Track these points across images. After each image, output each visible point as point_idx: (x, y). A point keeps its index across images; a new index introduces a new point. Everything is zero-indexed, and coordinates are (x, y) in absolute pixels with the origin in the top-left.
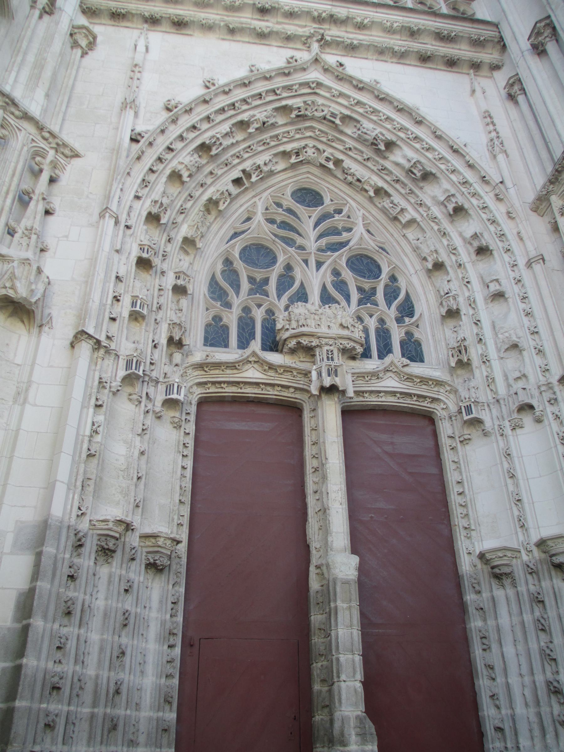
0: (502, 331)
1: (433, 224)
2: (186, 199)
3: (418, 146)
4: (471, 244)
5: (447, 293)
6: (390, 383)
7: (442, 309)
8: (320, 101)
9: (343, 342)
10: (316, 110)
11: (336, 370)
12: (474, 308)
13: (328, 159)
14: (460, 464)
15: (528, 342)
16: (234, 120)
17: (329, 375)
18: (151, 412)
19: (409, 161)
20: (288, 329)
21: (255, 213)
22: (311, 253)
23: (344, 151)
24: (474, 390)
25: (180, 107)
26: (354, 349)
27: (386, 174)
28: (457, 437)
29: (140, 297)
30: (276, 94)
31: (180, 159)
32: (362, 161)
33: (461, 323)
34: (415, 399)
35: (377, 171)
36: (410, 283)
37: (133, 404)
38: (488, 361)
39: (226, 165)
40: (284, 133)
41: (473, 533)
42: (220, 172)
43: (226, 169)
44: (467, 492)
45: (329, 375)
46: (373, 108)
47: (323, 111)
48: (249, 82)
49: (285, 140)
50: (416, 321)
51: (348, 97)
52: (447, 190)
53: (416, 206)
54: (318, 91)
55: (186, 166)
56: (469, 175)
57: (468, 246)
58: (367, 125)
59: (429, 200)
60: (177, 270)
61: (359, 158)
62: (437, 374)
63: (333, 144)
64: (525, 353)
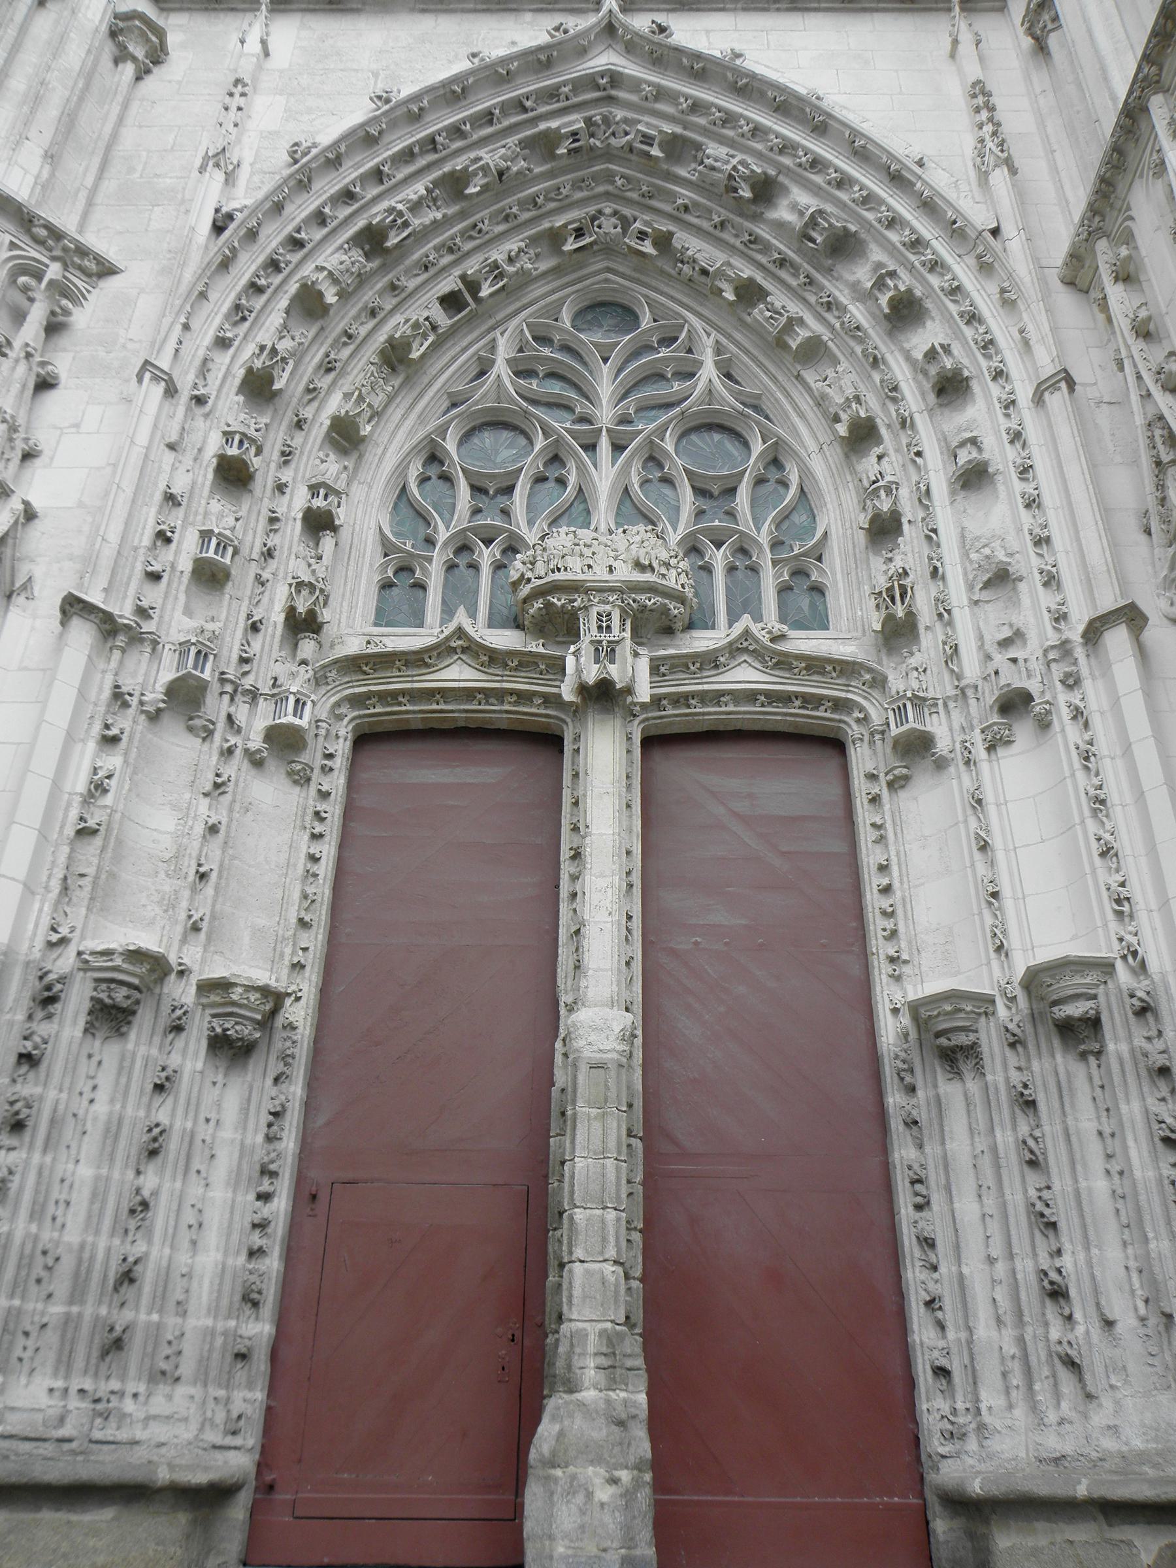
0: (978, 545)
1: (852, 343)
2: (336, 341)
3: (818, 179)
4: (925, 373)
6: (746, 675)
7: (862, 516)
8: (619, 114)
9: (642, 597)
10: (613, 134)
11: (613, 650)
12: (927, 507)
13: (642, 236)
15: (1028, 563)
16: (436, 174)
17: (597, 661)
18: (238, 752)
19: (801, 214)
20: (529, 580)
21: (493, 362)
22: (600, 429)
23: (675, 213)
24: (915, 674)
25: (314, 151)
26: (665, 611)
27: (759, 251)
28: (882, 775)
29: (216, 531)
30: (525, 110)
31: (320, 262)
32: (711, 229)
34: (798, 703)
35: (742, 247)
36: (806, 473)
37: (197, 736)
39: (426, 268)
40: (547, 191)
42: (412, 284)
43: (425, 276)
44: (896, 885)
45: (597, 661)
46: (727, 112)
47: (626, 134)
48: (463, 90)
49: (552, 205)
50: (815, 546)
51: (671, 96)
52: (879, 265)
53: (819, 309)
54: (614, 92)
55: (331, 273)
56: (925, 228)
57: (920, 377)
58: (714, 150)
59: (846, 292)
60: (314, 481)
61: (706, 225)
62: (846, 650)
63: (654, 203)
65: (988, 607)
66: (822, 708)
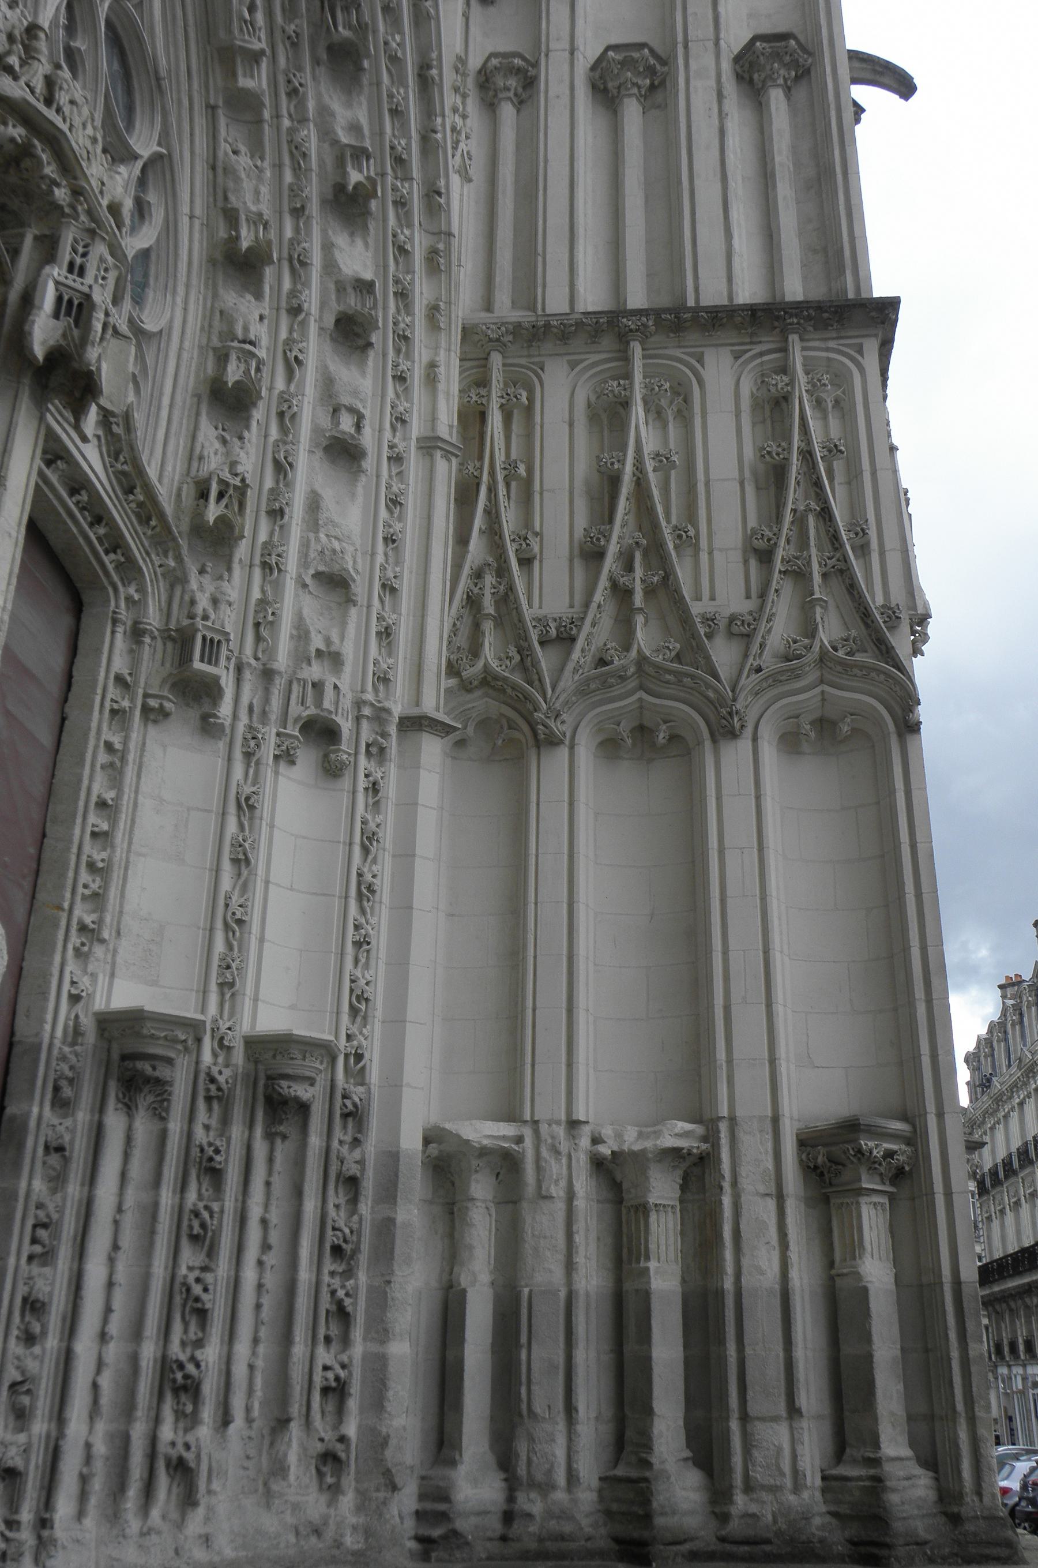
1: (287, 160)
4: (340, 288)
5: (251, 343)
14: (123, 759)
33: (246, 434)
38: (280, 570)
41: (99, 951)
44: (119, 837)
53: (281, 79)
64: (353, 612)
65: (308, 597)
66: (112, 556)
